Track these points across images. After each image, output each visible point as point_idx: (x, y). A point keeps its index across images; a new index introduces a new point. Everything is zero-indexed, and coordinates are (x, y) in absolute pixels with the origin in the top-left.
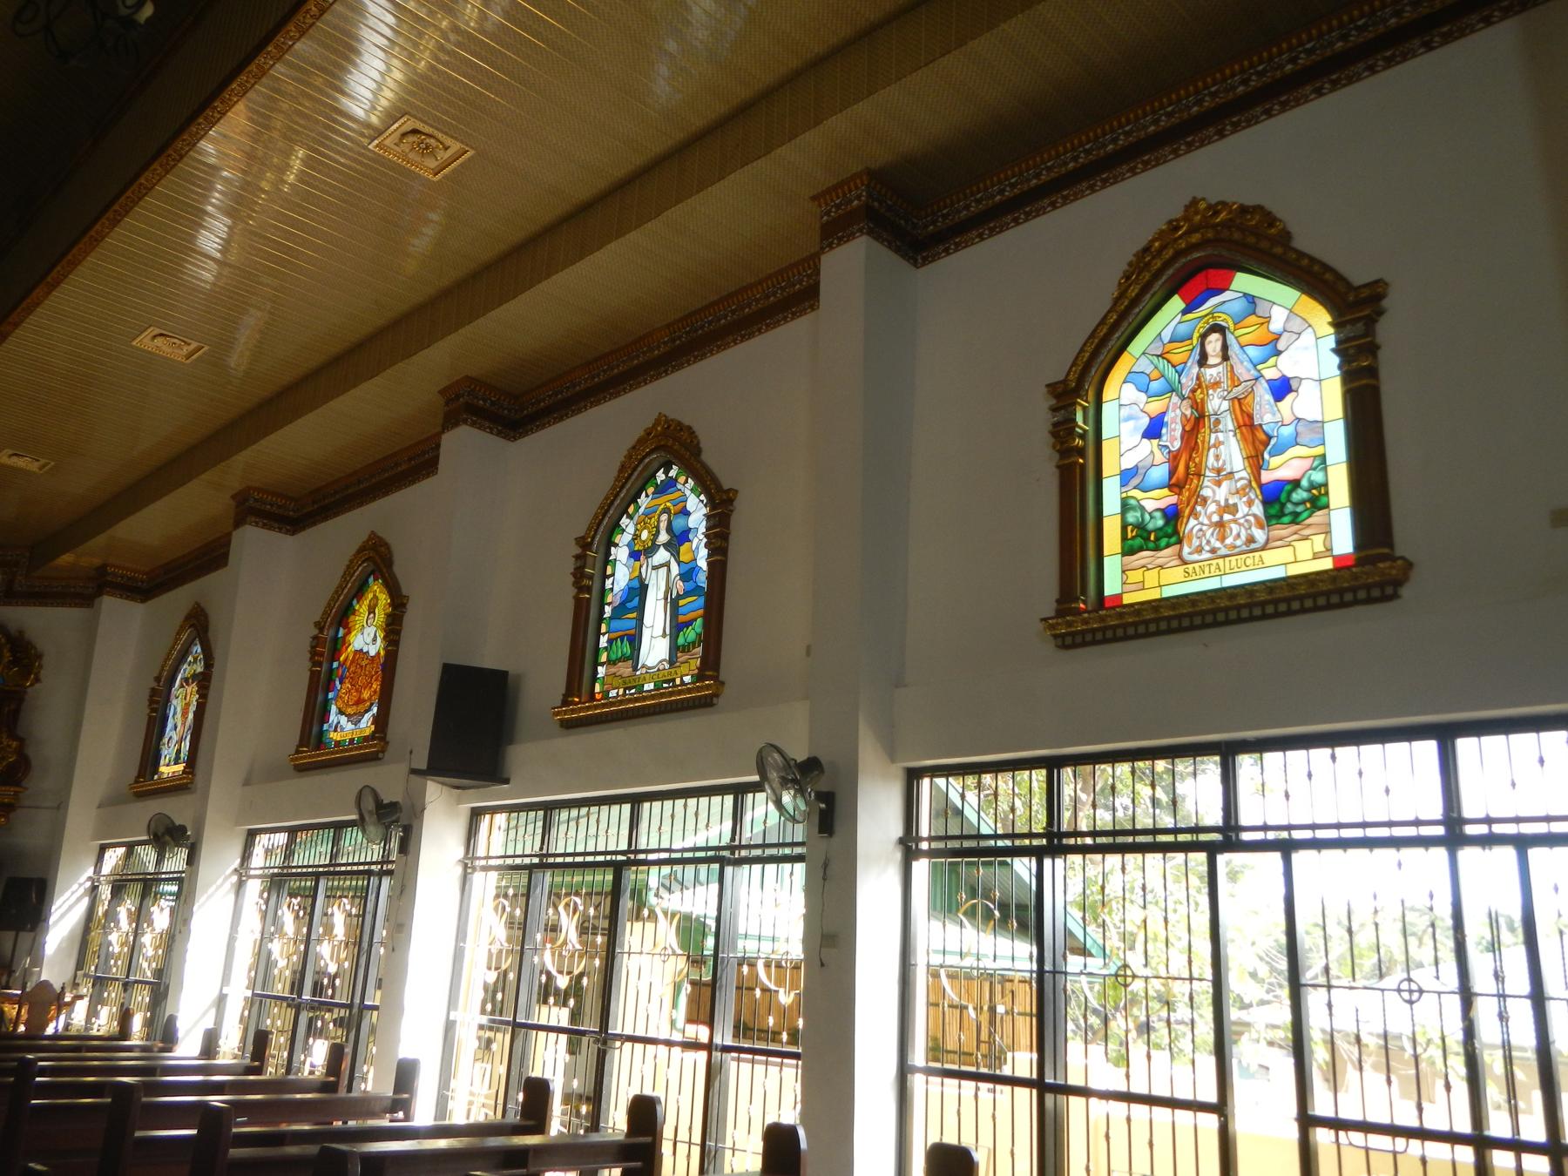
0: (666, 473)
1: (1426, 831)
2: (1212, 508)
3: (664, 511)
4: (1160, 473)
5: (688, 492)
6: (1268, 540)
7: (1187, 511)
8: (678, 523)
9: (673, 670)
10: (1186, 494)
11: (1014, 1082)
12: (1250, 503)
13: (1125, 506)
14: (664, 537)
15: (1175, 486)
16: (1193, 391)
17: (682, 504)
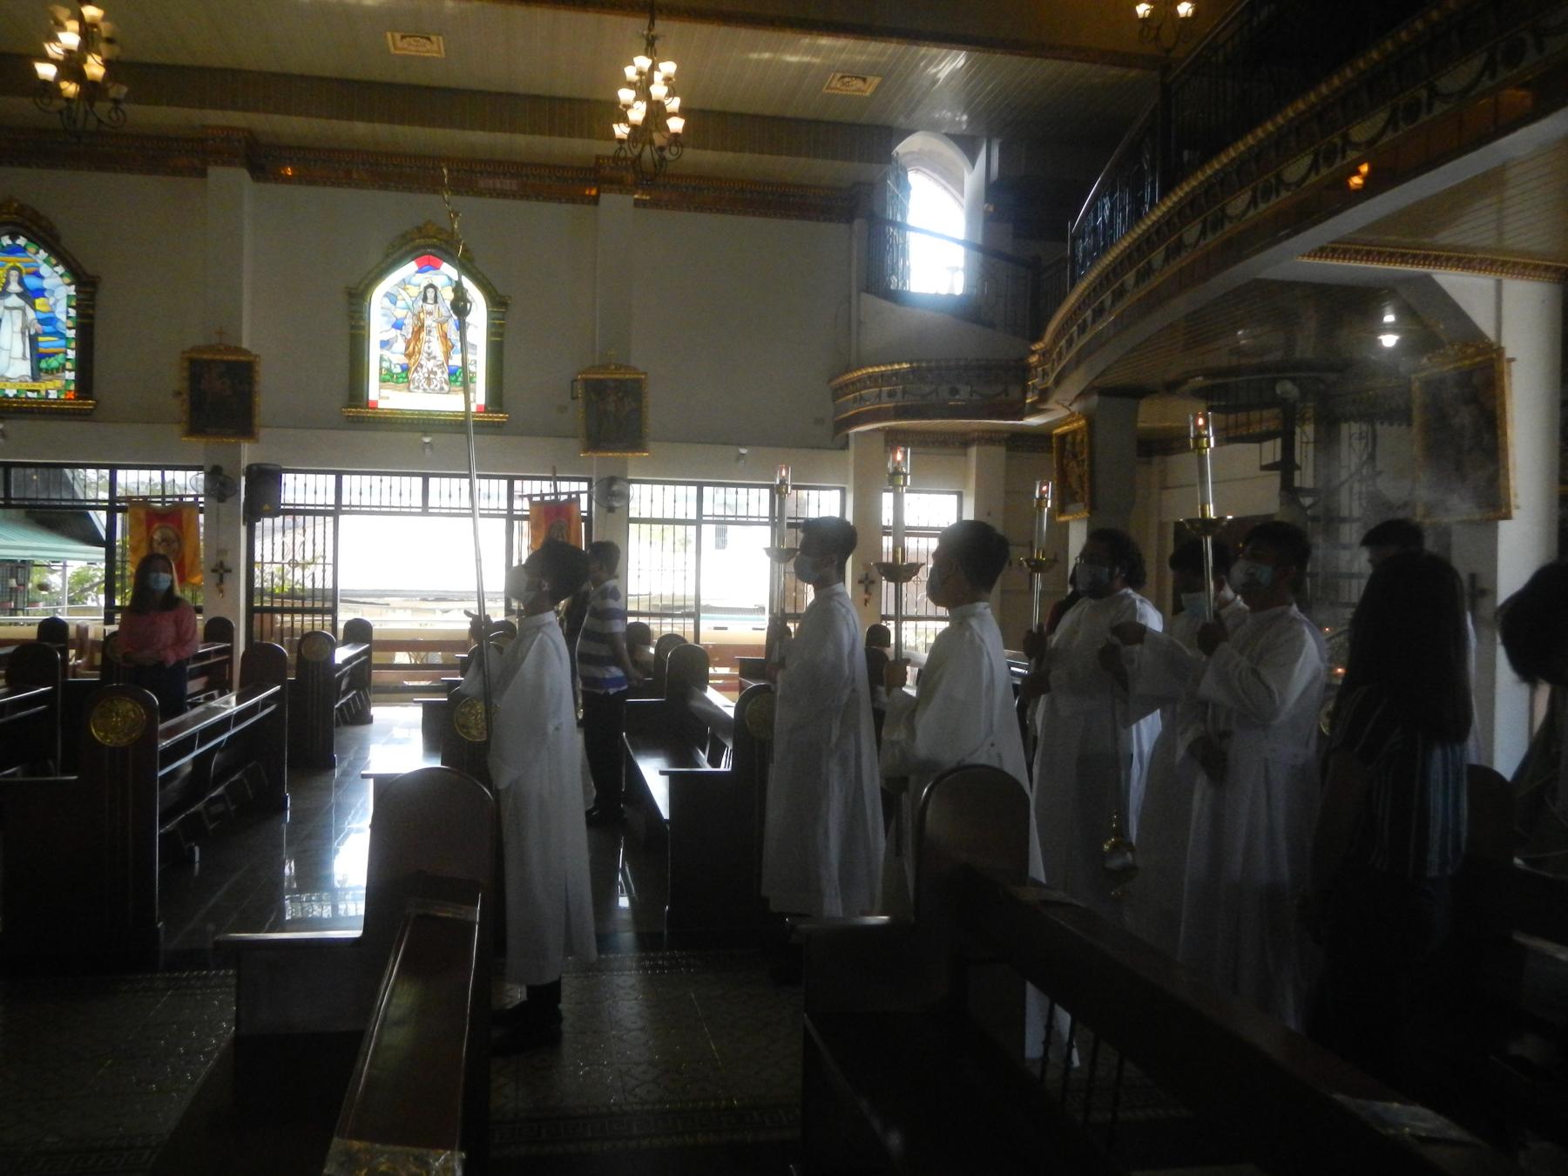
0: (14, 237)
1: (501, 512)
2: (425, 370)
3: (15, 268)
4: (400, 346)
5: (40, 262)
6: (449, 391)
7: (413, 369)
8: (32, 282)
9: (37, 384)
10: (413, 361)
11: (282, 619)
12: (443, 373)
13: (382, 359)
14: (14, 287)
15: (409, 356)
16: (419, 313)
17: (32, 269)
